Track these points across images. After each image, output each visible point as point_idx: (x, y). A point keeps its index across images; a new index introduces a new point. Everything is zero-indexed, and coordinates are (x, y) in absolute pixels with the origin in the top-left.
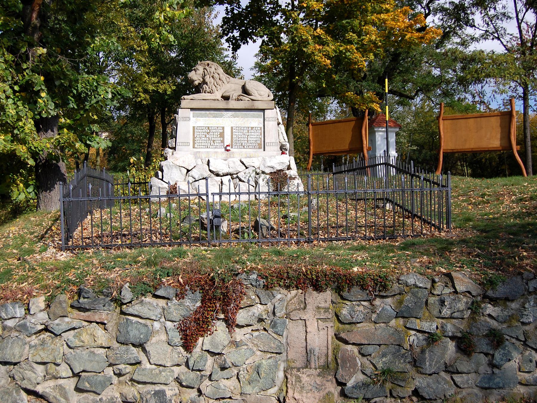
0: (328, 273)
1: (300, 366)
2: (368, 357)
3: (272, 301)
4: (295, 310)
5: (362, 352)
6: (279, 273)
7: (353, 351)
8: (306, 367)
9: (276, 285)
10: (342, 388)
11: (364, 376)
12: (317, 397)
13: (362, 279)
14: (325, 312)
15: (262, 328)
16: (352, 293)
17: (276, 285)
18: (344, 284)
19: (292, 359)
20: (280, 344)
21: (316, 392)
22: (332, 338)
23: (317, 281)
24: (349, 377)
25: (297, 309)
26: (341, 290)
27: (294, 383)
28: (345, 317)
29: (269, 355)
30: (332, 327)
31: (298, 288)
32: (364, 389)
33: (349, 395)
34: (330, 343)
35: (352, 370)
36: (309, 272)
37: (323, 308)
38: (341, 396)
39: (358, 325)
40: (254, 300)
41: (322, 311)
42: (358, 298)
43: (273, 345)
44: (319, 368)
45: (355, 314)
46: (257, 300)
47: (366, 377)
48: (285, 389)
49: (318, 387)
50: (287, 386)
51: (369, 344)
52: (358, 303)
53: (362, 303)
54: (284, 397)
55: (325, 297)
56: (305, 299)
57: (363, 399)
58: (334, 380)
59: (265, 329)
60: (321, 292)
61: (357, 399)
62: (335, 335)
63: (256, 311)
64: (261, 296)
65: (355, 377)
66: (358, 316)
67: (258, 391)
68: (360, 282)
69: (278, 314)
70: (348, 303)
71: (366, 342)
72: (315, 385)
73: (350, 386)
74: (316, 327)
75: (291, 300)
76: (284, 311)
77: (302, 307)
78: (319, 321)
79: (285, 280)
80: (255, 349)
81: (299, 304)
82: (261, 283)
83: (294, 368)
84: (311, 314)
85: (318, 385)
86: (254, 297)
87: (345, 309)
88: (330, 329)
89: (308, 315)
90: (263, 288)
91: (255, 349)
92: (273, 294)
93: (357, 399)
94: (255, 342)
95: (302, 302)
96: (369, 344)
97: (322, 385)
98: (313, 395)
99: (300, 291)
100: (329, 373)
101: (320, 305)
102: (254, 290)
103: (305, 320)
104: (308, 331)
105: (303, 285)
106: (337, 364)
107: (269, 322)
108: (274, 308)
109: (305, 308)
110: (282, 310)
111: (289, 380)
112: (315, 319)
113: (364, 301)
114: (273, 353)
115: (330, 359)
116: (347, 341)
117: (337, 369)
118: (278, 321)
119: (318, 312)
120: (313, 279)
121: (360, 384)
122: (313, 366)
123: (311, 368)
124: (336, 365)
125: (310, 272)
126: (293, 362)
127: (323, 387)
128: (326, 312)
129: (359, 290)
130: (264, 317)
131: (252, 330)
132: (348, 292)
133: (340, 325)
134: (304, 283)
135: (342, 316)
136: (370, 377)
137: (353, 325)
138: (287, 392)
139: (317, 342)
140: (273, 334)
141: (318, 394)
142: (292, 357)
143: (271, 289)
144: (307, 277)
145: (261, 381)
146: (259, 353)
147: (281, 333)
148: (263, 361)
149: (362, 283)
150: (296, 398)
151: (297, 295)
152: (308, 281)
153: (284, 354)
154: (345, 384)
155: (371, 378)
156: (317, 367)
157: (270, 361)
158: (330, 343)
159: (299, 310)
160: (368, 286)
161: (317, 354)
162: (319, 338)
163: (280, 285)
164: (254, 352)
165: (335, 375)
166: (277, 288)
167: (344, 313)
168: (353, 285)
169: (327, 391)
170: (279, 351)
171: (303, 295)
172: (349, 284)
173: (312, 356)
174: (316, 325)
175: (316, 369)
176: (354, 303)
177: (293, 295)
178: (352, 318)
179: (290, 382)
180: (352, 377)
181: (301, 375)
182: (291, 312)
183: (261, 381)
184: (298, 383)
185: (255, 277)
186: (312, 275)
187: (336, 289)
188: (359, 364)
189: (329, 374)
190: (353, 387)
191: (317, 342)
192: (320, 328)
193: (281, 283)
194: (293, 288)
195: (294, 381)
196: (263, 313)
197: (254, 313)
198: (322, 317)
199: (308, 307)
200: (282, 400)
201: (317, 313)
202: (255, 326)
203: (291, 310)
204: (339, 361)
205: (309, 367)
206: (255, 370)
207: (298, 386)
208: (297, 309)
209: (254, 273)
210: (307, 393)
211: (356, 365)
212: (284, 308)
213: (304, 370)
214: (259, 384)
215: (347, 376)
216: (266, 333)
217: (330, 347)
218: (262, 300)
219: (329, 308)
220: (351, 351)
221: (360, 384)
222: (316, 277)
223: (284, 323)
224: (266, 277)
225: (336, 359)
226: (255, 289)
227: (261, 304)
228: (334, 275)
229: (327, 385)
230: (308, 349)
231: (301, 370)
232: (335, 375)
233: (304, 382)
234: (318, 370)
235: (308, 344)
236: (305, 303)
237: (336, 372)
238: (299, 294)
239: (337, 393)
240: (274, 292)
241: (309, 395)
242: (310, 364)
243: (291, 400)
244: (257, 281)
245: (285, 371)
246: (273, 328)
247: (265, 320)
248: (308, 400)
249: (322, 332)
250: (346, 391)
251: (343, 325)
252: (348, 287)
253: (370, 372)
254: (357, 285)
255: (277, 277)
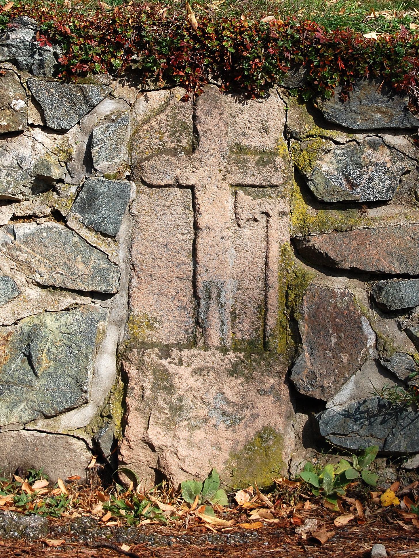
0: (275, 34)
1: (172, 340)
2: (402, 319)
3: (85, 120)
4: (160, 152)
5: (382, 299)
6: (111, 27)
7: (351, 296)
8: (193, 343)
9: (98, 67)
10: (311, 417)
11: (386, 380)
12: (227, 445)
13: (388, 57)
14: (262, 163)
15: (49, 211)
16: (354, 105)
17: (98, 67)
18: (326, 72)
19: (145, 315)
20: (104, 265)
21: (222, 426)
22: (284, 251)
23: (237, 58)
24: (335, 382)
25: (167, 152)
26: (318, 94)
27: (148, 393)
28: (326, 182)
29: (68, 300)
30: (282, 214)
31: (171, 84)
32: (382, 423)
33: (335, 440)
34: (274, 265)
35: (345, 358)
36: (210, 29)
37: (255, 152)
38: (306, 446)
39: (372, 213)
40: (23, 113)
41: (252, 160)
42: (373, 121)
43: (81, 266)
44: (235, 350)
45: (362, 175)
46: (34, 117)
47: (391, 383)
48: (117, 412)
49: (229, 410)
50: (125, 405)
51: (405, 276)
52: (373, 138)
53: (388, 138)
54: (115, 441)
55: (264, 116)
56: (194, 117)
57: (380, 455)
58: (285, 391)
59: (57, 216)
60: (248, 98)
61: (360, 453)
62: (294, 241)
63: (27, 152)
64: (46, 102)
65: (356, 383)
66: (371, 180)
67: (26, 418)
68: (383, 69)
69: (101, 165)
70: (341, 137)
71: (396, 268)
72: (221, 404)
73: (338, 409)
74: (230, 214)
75: (147, 121)
76: (124, 155)
77: (184, 143)
78: (241, 193)
79: (129, 52)
80: (21, 278)
81: (173, 134)
82: (48, 57)
83: (153, 345)
84: (214, 170)
85: (229, 403)
86: (21, 104)
87: (328, 157)
88: (275, 221)
89: (202, 173)
90: (55, 75)
91: (21, 278)
92: (86, 98)
93: (360, 453)
94: (23, 257)
95: (184, 127)
96: (405, 276)
97: (244, 407)
98: (212, 437)
99: (180, 92)
100: (268, 364)
101: (245, 142)
102: (24, 79)
103: (192, 188)
104: (202, 221)
105: (189, 70)
106: (297, 337)
107: (73, 190)
108: (90, 145)
109: (194, 148)
110: (116, 150)
111: (131, 384)
112: (225, 185)
113: (395, 131)
114: (81, 293)
115: (272, 321)
116: (334, 262)
117: (298, 352)
118: (102, 189)
119: (237, 162)
120: (223, 50)
121: (373, 406)
122: (214, 339)
123: (206, 347)
124: (291, 342)
125: (216, 31)
126: (150, 326)
127: (248, 413)
128: (265, 164)
129: (379, 96)
130: (56, 173)
131: (15, 218)
132: (342, 100)
133: (311, 211)
134: (194, 66)
135: (318, 179)
136: (404, 383)
137: (357, 213)
138: (124, 422)
139: (230, 261)
140: (84, 232)
141: (229, 434)
142: (147, 310)
143: (78, 80)
144: (204, 46)
145: (38, 384)
146: (34, 292)
147: (110, 230)
148: (49, 319)
149: (388, 71)
150: (155, 443)
151: (167, 104)
152: (206, 61)
153: (121, 299)
154: (321, 406)
155: (407, 387)
156: (229, 343)
157: (69, 318)
158: (274, 265)
159: (174, 152)
160: (408, 80)
161: (230, 303)
162: (238, 247)
163: (111, 69)
164: (16, 288)
165: (289, 373)
166: (103, 79)
167: (325, 168)
168: (358, 76)
169: (259, 425)
170: (101, 288)
171: (188, 104)
172: (343, 73)
173: (214, 306)
174: (230, 205)
175: (224, 350)
176: (360, 137)
177: (156, 106)
178: (353, 186)
179: (137, 390)
180: (347, 380)
181: (172, 369)
182: (148, 159)
183: (38, 384)
184: (162, 395)
185: (28, 38)
186: (220, 39)
187: (301, 92)
188: (371, 341)
189: (269, 371)
190: (347, 415)
191: (230, 261)
192: (244, 215)
193: (116, 63)
194: (156, 81)
195: (148, 386)
196: (52, 160)
197: (22, 159)
198: (250, 180)
199: (204, 144)
200: (107, 452)
201: (233, 167)
202: (25, 204)
203: (149, 153)
204: (304, 328)
205: (200, 344)
206: (15, 350)
207: (161, 402)
208: (167, 152)
209: (25, 24)
210: (192, 428)
211: (361, 340)
212: (124, 148)
213: (186, 353)
214: (31, 395)
215: (328, 375)
216: (60, 226)
217: (274, 280)
218: (49, 114)
219: (274, 153)
220: (343, 295)
221: (373, 406)
222: (236, 45)
223: (123, 194)
224: (65, 36)
225: (293, 322)
226: (25, 77)
227: (45, 128)
228: (296, 42)
229: (260, 405)
230: (200, 285)
231: (175, 352)
232: (289, 373)
233: (181, 392)
234: (232, 355)
235: (201, 269)
236: (196, 131)
237: (293, 364)
238: (176, 101)
239: (292, 435)
240: (92, 90)
241: (200, 435)
242: (204, 333)
243: (137, 449)
244: (32, 49)
245: (120, 356)
246: (83, 210)
247: (59, 185)
248: (195, 453)
249: (247, 231)
250: (322, 427)
251: (321, 212)
252: (341, 84)
253: (404, 366)
254: (372, 76)
255: (102, 41)
